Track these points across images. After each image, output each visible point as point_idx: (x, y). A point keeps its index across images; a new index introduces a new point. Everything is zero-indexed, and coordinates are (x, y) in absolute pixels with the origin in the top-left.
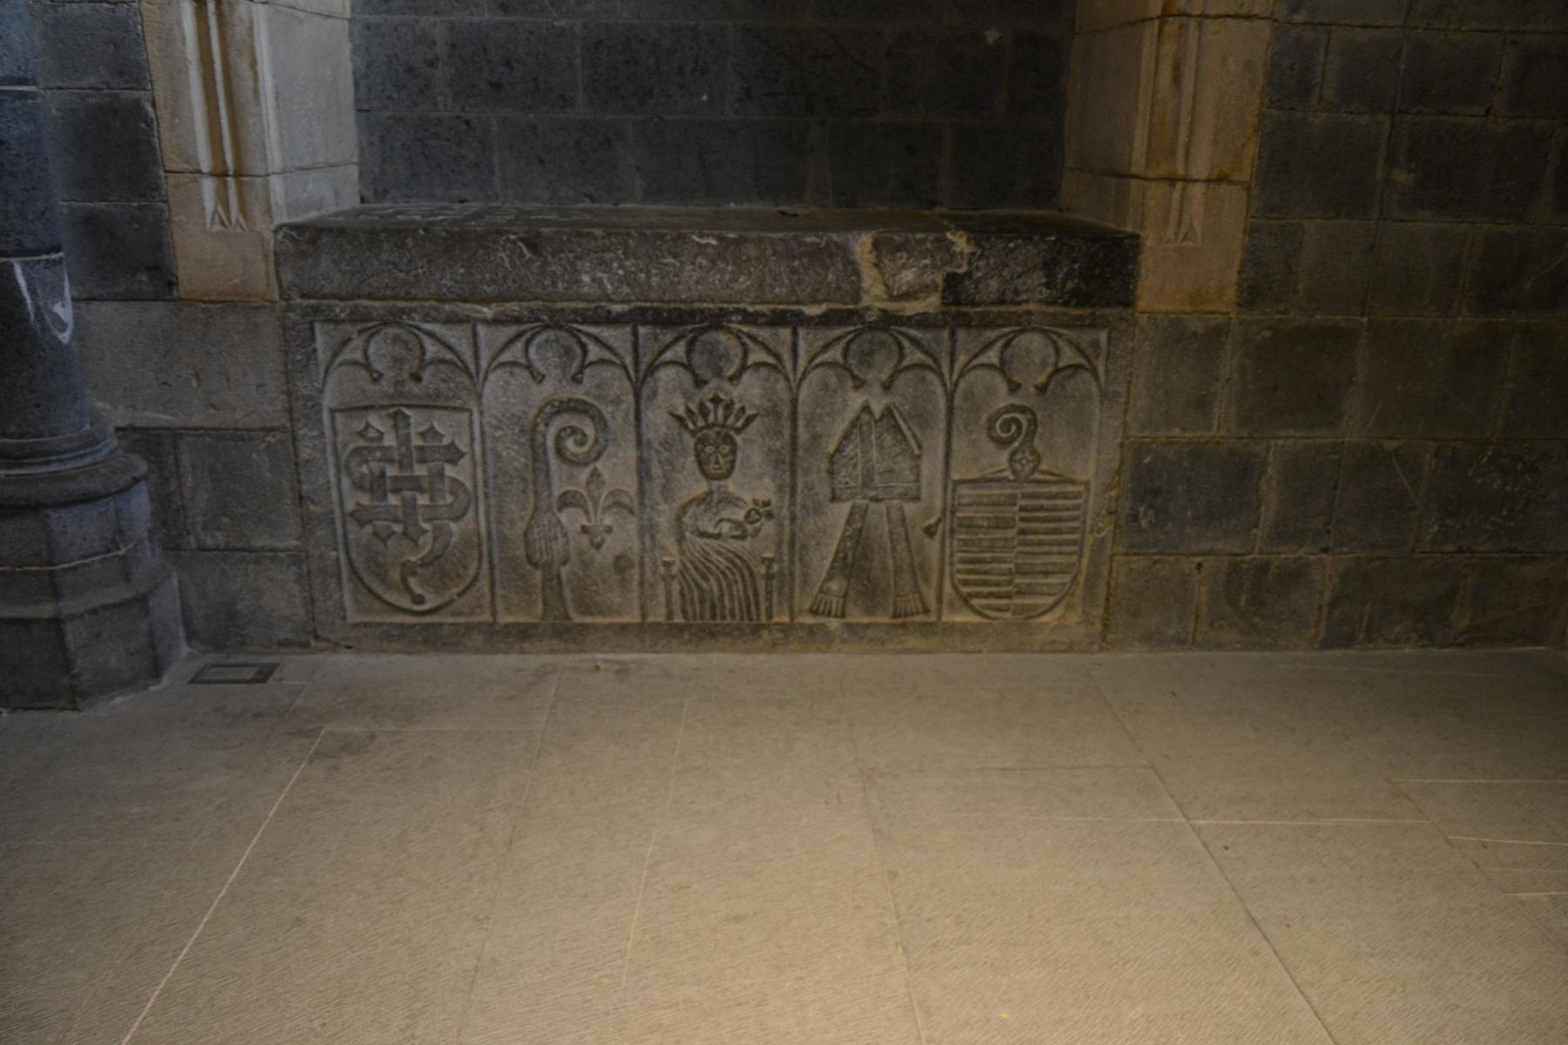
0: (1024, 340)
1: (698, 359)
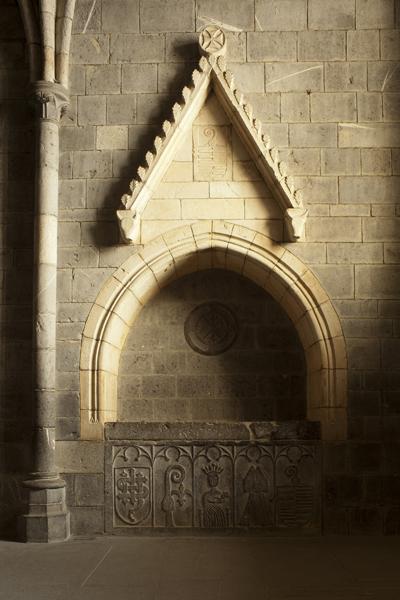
0: (292, 448)
1: (208, 455)
